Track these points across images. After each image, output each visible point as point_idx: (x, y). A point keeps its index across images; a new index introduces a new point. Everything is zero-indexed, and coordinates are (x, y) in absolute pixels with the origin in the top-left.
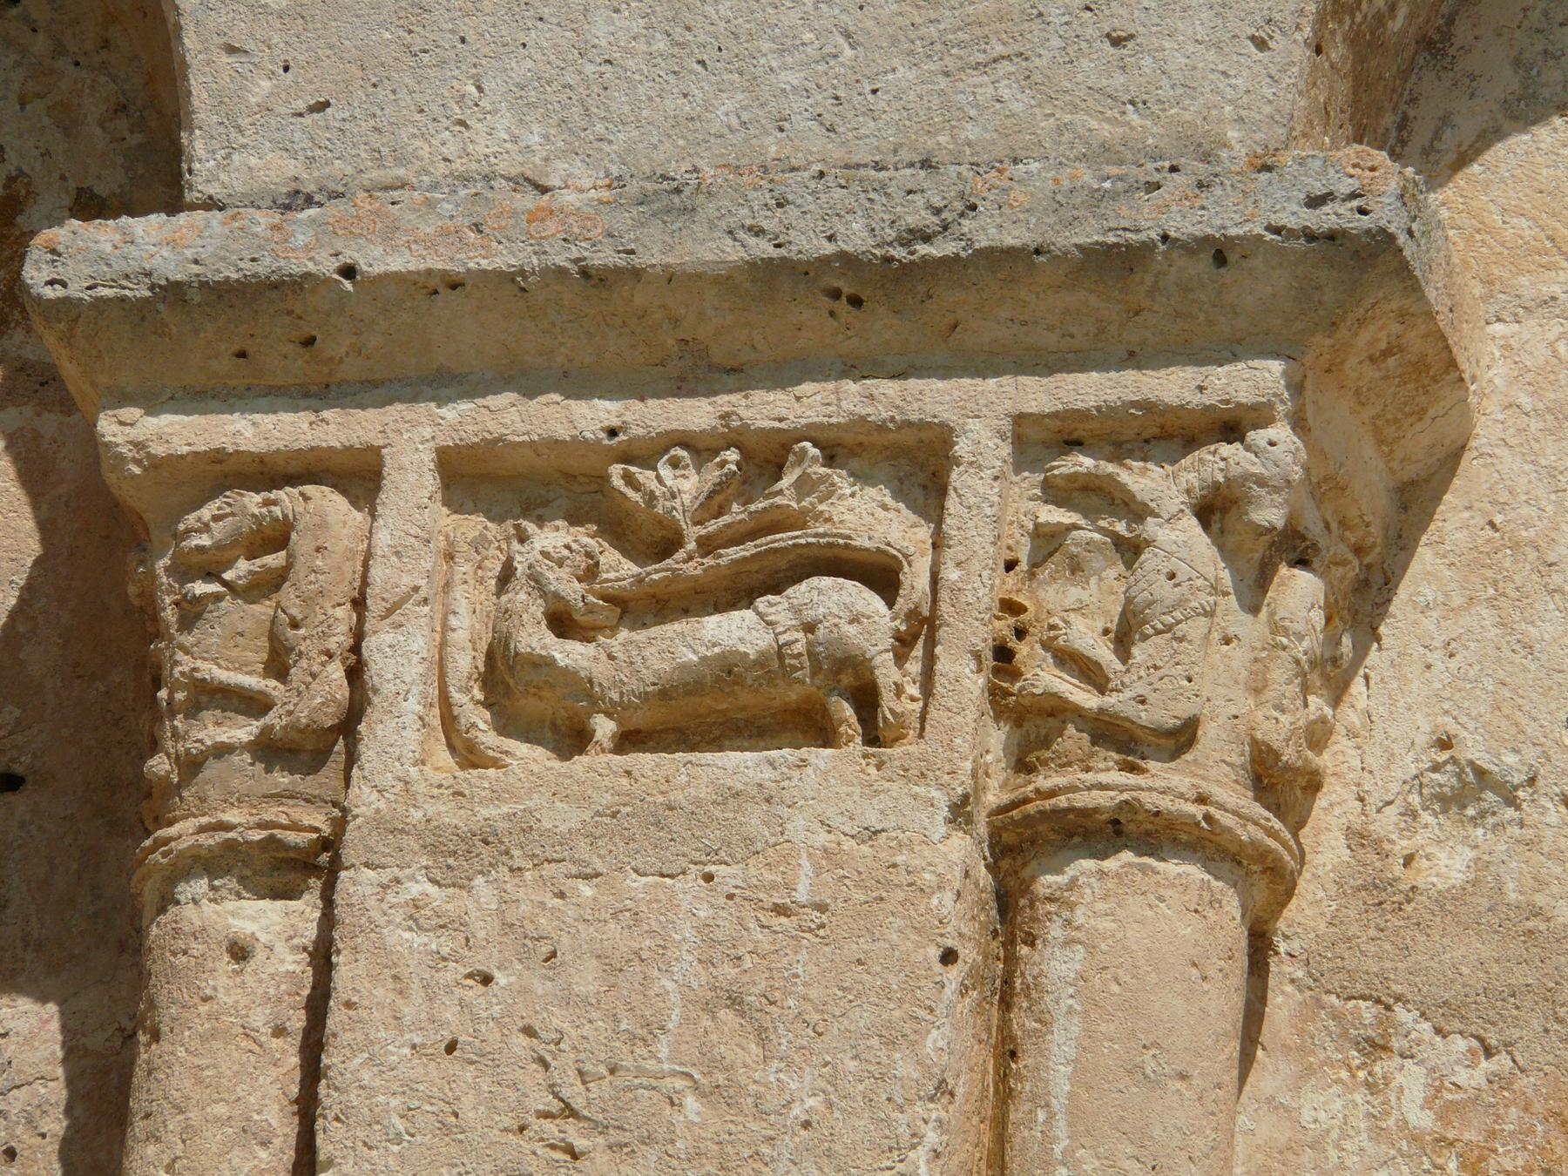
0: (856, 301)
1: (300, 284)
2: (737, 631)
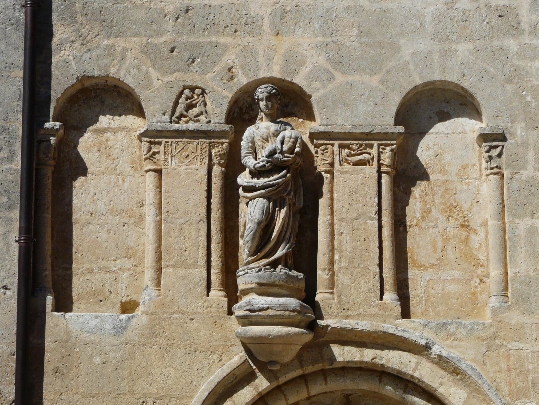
2: (360, 157)
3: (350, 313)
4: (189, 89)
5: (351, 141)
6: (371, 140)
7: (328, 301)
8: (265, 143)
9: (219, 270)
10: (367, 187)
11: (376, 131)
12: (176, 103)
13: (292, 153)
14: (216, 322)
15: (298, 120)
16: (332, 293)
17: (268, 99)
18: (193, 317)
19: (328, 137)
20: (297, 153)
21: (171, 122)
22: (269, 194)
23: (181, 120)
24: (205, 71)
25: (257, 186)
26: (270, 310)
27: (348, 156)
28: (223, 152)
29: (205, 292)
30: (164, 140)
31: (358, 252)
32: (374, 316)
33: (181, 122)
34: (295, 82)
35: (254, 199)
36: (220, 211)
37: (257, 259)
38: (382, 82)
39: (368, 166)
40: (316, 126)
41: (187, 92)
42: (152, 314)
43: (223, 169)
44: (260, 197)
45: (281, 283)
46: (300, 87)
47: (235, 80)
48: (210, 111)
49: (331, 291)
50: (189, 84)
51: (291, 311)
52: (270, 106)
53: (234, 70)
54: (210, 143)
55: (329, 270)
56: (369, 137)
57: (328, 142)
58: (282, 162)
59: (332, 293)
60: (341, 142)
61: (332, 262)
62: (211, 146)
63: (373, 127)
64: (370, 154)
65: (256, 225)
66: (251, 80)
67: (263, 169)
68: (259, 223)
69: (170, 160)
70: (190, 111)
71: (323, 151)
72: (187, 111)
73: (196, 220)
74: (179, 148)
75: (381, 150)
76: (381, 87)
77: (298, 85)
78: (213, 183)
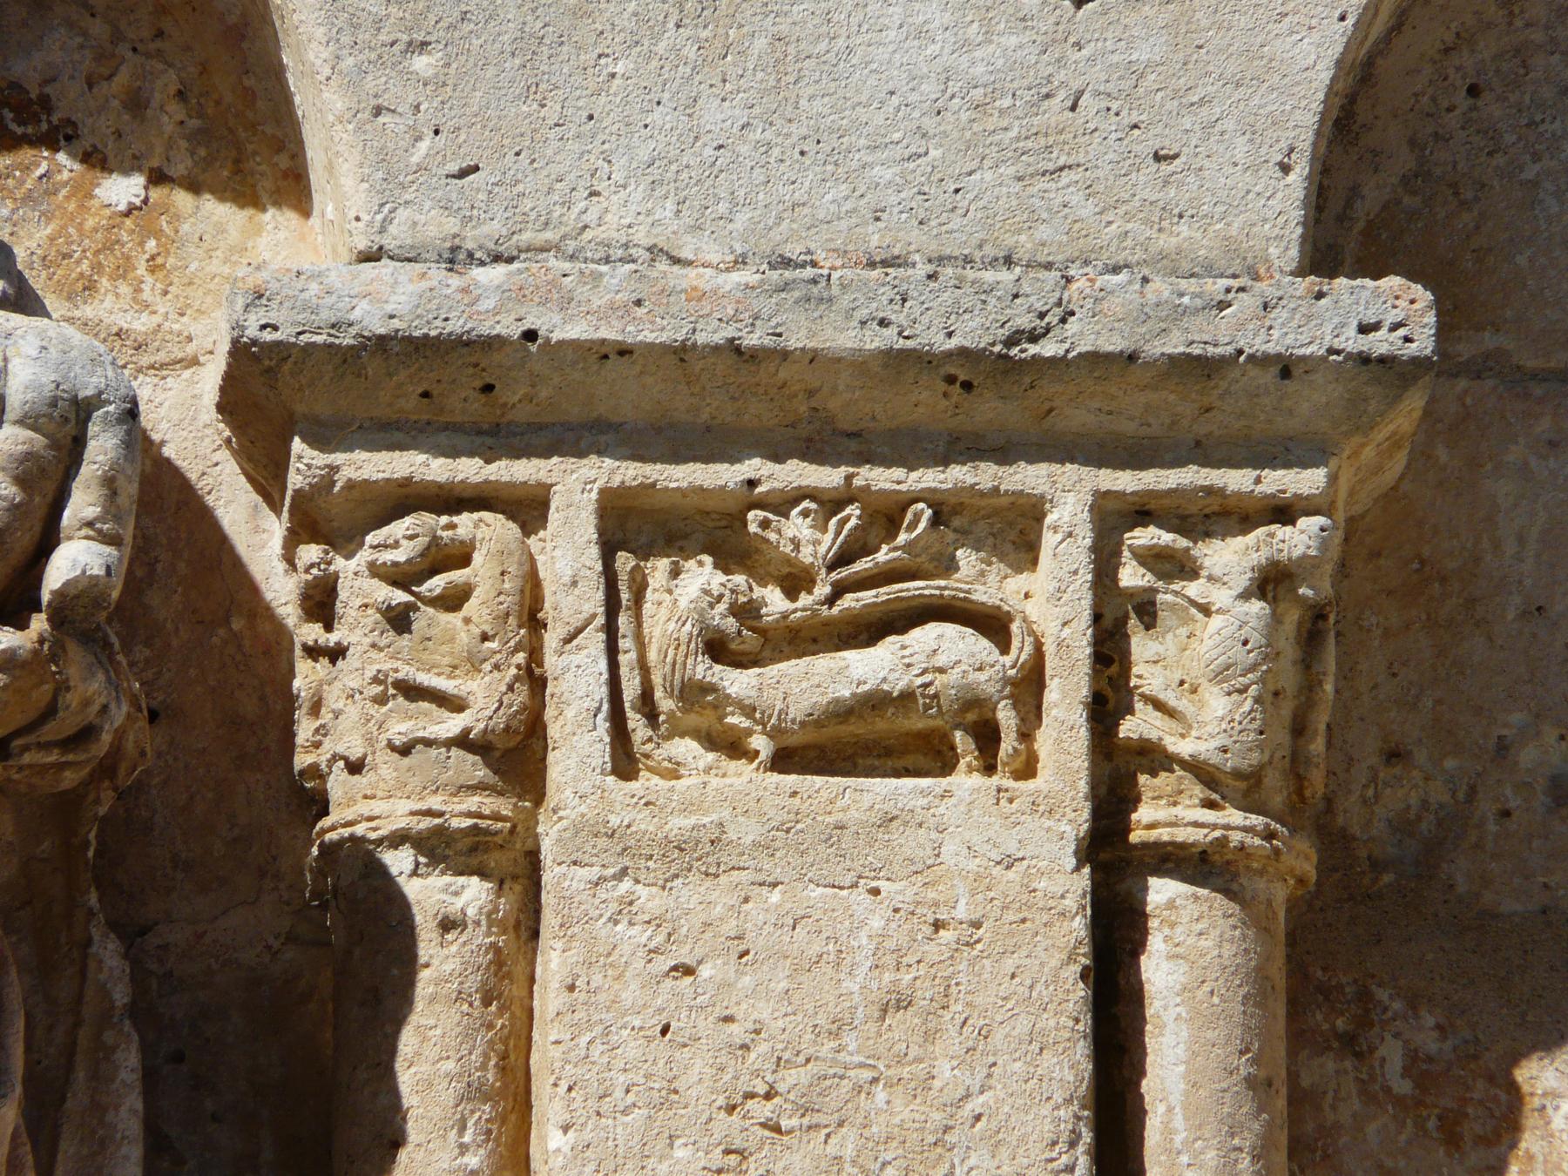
0: (967, 386)
1: (493, 343)
5: (753, 467)
6: (1004, 454)
10: (952, 1041)
11: (1081, 336)
15: (83, 193)
19: (463, 403)
20: (77, 613)
27: (717, 648)
39: (966, 781)
40: (314, 265)
56: (989, 410)
57: (469, 470)
60: (630, 472)
63: (1041, 290)
71: (401, 577)
75: (1131, 576)
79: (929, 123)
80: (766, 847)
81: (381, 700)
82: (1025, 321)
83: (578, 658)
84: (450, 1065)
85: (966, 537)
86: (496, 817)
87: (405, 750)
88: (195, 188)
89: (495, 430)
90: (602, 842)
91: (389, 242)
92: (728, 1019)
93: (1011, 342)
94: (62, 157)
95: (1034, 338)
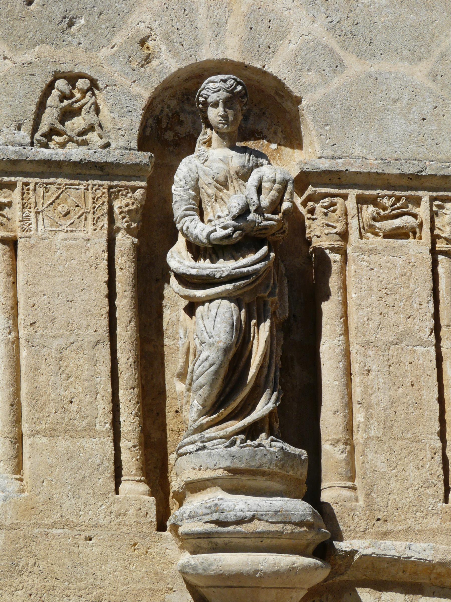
0: (411, 179)
1: (341, 171)
2: (398, 222)
3: (389, 527)
4: (64, 78)
6: (416, 189)
7: (348, 504)
8: (220, 190)
9: (136, 442)
10: (412, 281)
11: (428, 172)
12: (42, 106)
13: (275, 212)
14: (135, 544)
15: (268, 146)
16: (354, 488)
17: (227, 103)
18: (91, 533)
19: (336, 181)
21: (32, 144)
22: (240, 292)
23: (51, 140)
24: (96, 43)
25: (217, 276)
26: (256, 522)
27: (374, 219)
28: (135, 206)
29: (113, 485)
30: (20, 180)
31: (401, 407)
32: (435, 532)
33: (51, 144)
34: (269, 70)
35: (210, 301)
36: (133, 324)
37: (217, 420)
38: (434, 76)
39: (411, 240)
41: (61, 84)
42: (12, 528)
43: (136, 241)
44: (223, 298)
45: (274, 469)
46: (280, 80)
47: (154, 63)
48: (108, 125)
49: (350, 484)
50: (66, 68)
51: (296, 524)
52: (231, 118)
53: (150, 43)
54: (110, 187)
55: (346, 444)
56: (414, 183)
57: (336, 191)
58: (261, 230)
59: (354, 488)
60: (360, 192)
61: (349, 428)
62: (113, 194)
63: (422, 164)
64: (415, 216)
65: (220, 354)
66: (185, 64)
67: (225, 242)
68: (226, 351)
69: (33, 220)
70: (68, 123)
71: (326, 208)
72: (62, 122)
73: (89, 342)
74: (49, 197)
75: (435, 209)
76: (430, 85)
77: (275, 78)
78: (117, 268)
79: (403, 138)
80: (383, 250)
81: (323, 227)
82: (420, 169)
83: (354, 221)
84: (336, 284)
85: (410, 202)
86: (342, 245)
87: (327, 235)
88: (285, 146)
89: (340, 185)
90: (359, 249)
91: (323, 156)
92: (379, 277)
93: (418, 172)
94: (264, 141)
95: (421, 172)
